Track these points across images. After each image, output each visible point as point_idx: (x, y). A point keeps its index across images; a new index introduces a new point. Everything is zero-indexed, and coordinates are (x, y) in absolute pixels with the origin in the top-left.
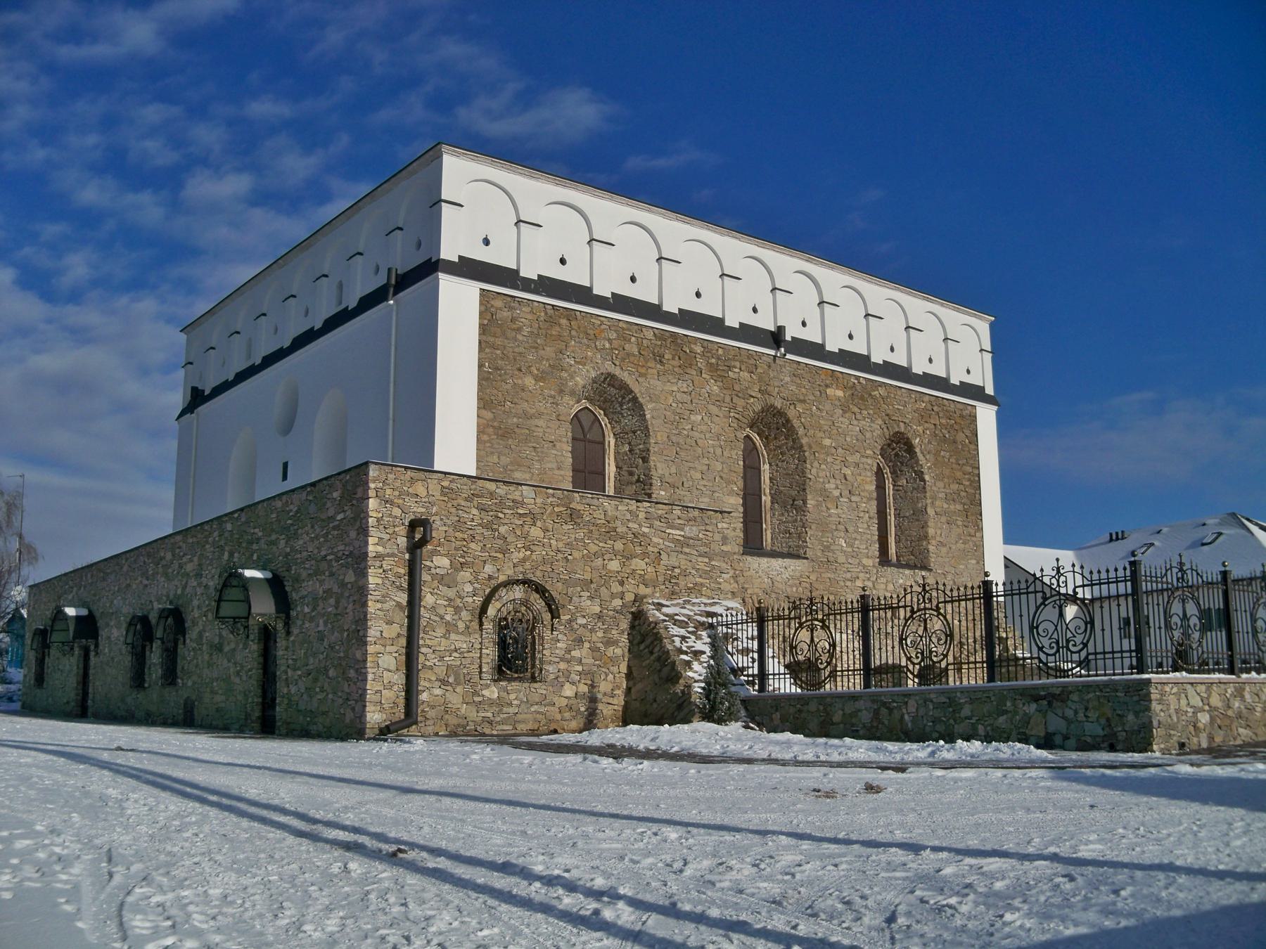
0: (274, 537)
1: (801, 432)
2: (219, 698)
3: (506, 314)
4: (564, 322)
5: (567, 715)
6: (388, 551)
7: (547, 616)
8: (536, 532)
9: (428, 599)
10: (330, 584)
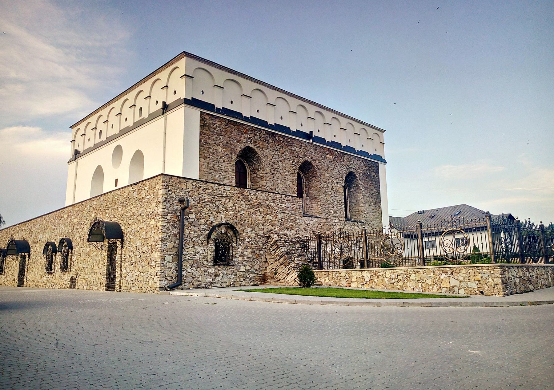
0: (116, 207)
1: (318, 171)
2: (87, 276)
4: (231, 126)
5: (242, 279)
6: (170, 211)
7: (234, 238)
8: (230, 204)
9: (187, 232)
10: (143, 225)
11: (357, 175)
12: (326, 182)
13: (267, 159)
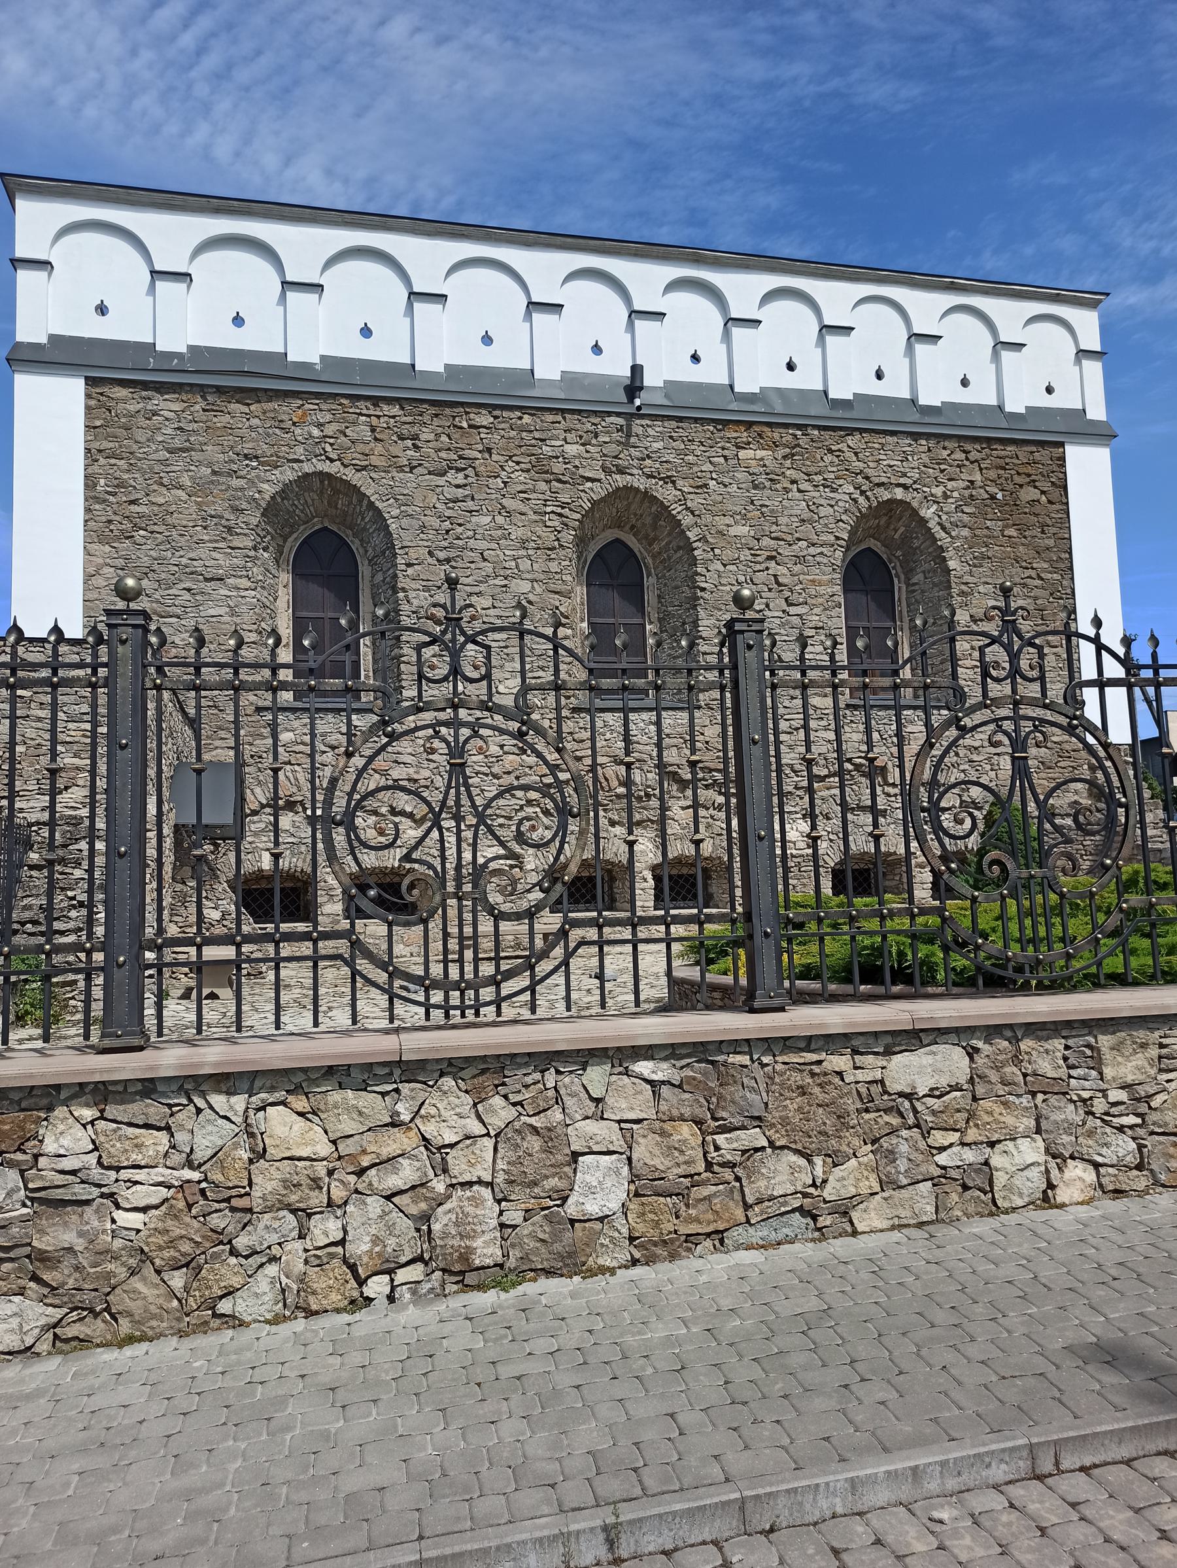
1: (687, 520)
3: (133, 407)
11: (928, 512)
12: (735, 561)
13: (410, 510)
